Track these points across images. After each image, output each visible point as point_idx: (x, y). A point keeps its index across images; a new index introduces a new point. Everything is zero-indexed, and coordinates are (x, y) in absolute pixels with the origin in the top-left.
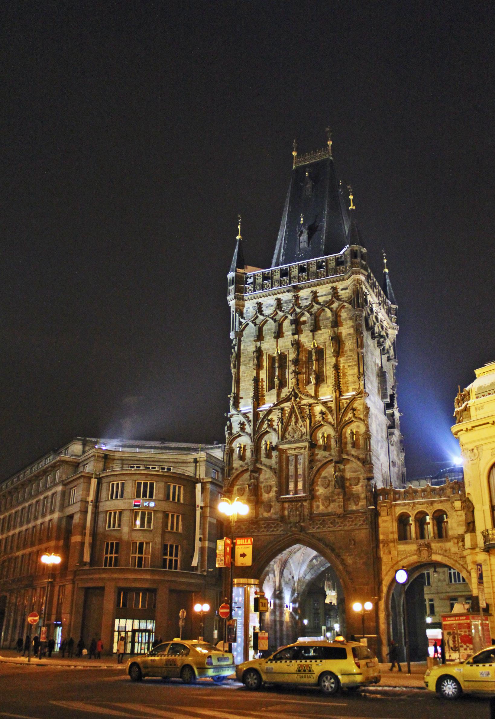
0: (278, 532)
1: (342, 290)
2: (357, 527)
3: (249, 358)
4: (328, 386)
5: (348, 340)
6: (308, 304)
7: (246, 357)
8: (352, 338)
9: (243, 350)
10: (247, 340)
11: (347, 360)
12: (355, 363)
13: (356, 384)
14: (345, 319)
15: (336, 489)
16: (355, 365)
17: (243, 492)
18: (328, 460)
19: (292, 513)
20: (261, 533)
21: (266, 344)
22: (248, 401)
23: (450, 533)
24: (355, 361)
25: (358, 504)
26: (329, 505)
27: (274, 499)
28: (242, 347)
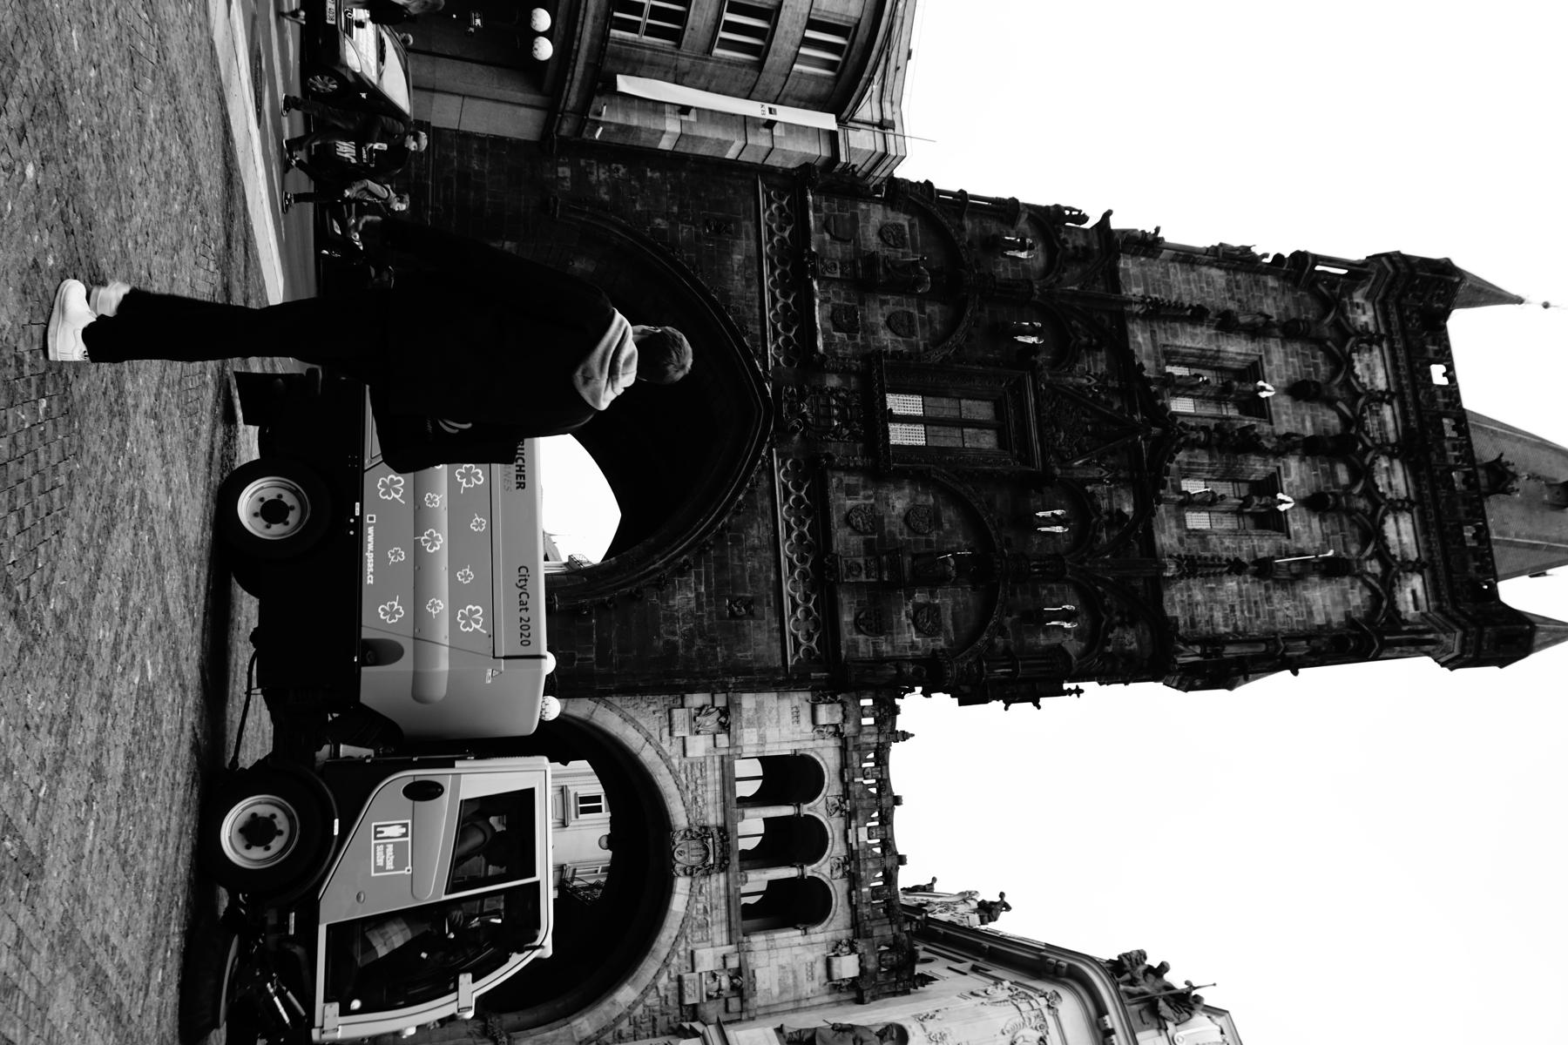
0: (771, 349)
1: (1414, 592)
2: (789, 626)
3: (1245, 300)
4: (1181, 541)
5: (1295, 607)
6: (1381, 490)
7: (1247, 293)
8: (1301, 619)
9: (1265, 286)
10: (1288, 298)
11: (1249, 601)
12: (1241, 629)
13: (1190, 630)
14: (1346, 601)
15: (910, 559)
16: (1235, 625)
17: (892, 242)
18: (993, 532)
19: (834, 402)
20: (769, 290)
21: (1282, 355)
22: (1137, 285)
23: (758, 941)
24: (1245, 628)
25: (860, 632)
26: (856, 530)
27: (874, 345)
28: (1271, 282)
